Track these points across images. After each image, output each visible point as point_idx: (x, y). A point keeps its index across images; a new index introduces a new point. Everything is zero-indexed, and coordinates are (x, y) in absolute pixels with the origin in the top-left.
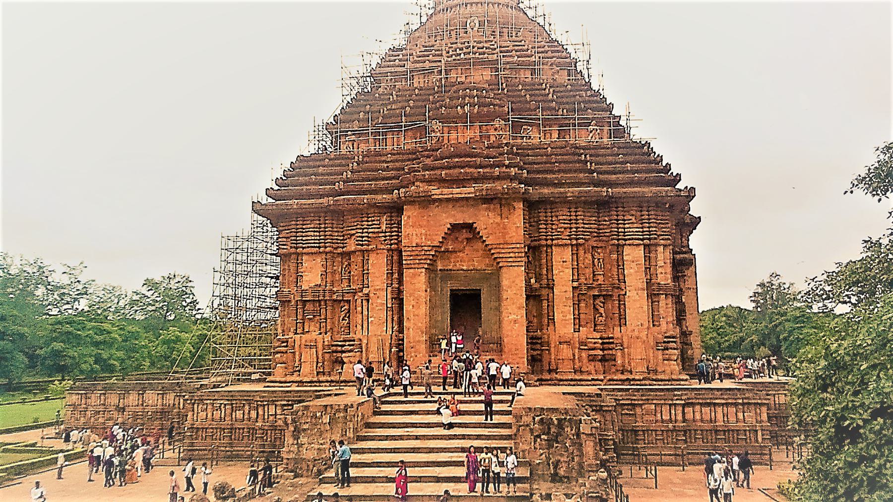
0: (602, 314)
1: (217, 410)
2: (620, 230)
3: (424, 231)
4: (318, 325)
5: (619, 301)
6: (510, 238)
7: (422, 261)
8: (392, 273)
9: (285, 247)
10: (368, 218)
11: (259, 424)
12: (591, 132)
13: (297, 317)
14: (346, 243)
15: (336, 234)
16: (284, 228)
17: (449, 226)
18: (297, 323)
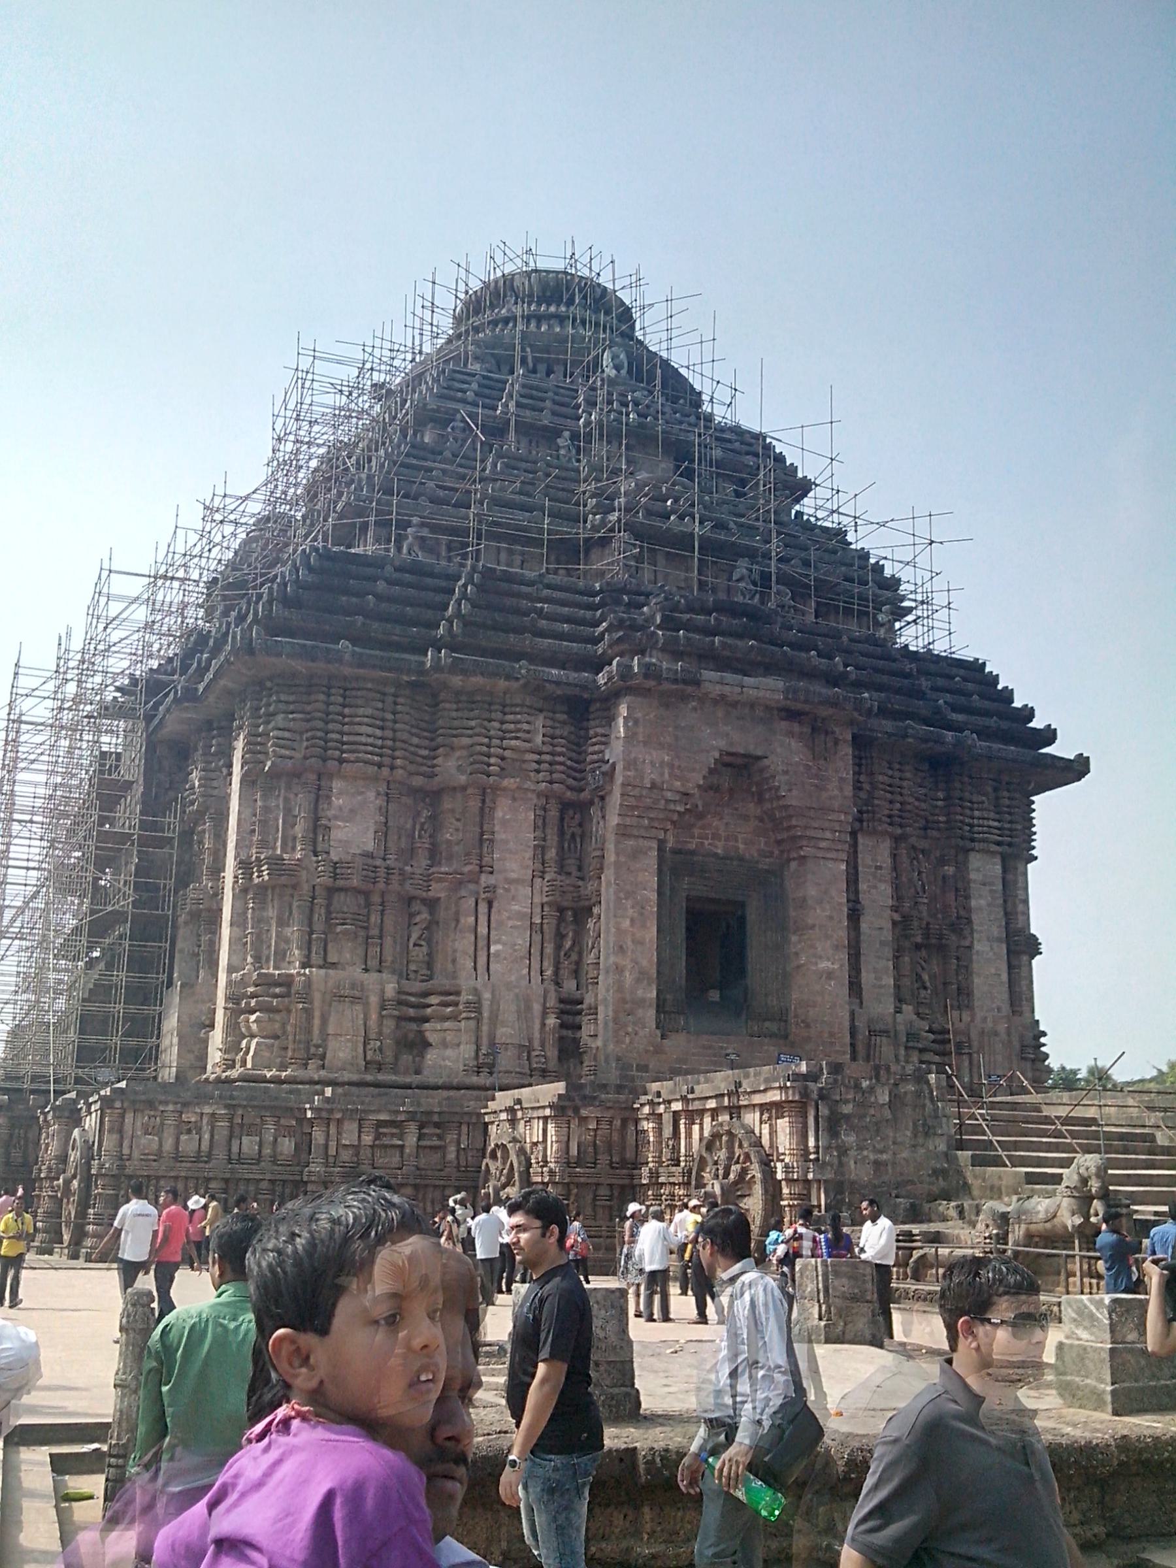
0: (923, 982)
1: (189, 1131)
2: (967, 820)
3: (666, 758)
4: (360, 951)
5: (958, 959)
6: (831, 798)
7: (656, 825)
8: (543, 849)
9: (287, 753)
10: (505, 714)
11: (316, 1168)
12: (882, 625)
13: (310, 925)
14: (434, 766)
15: (415, 740)
16: (292, 707)
17: (717, 755)
18: (310, 942)
